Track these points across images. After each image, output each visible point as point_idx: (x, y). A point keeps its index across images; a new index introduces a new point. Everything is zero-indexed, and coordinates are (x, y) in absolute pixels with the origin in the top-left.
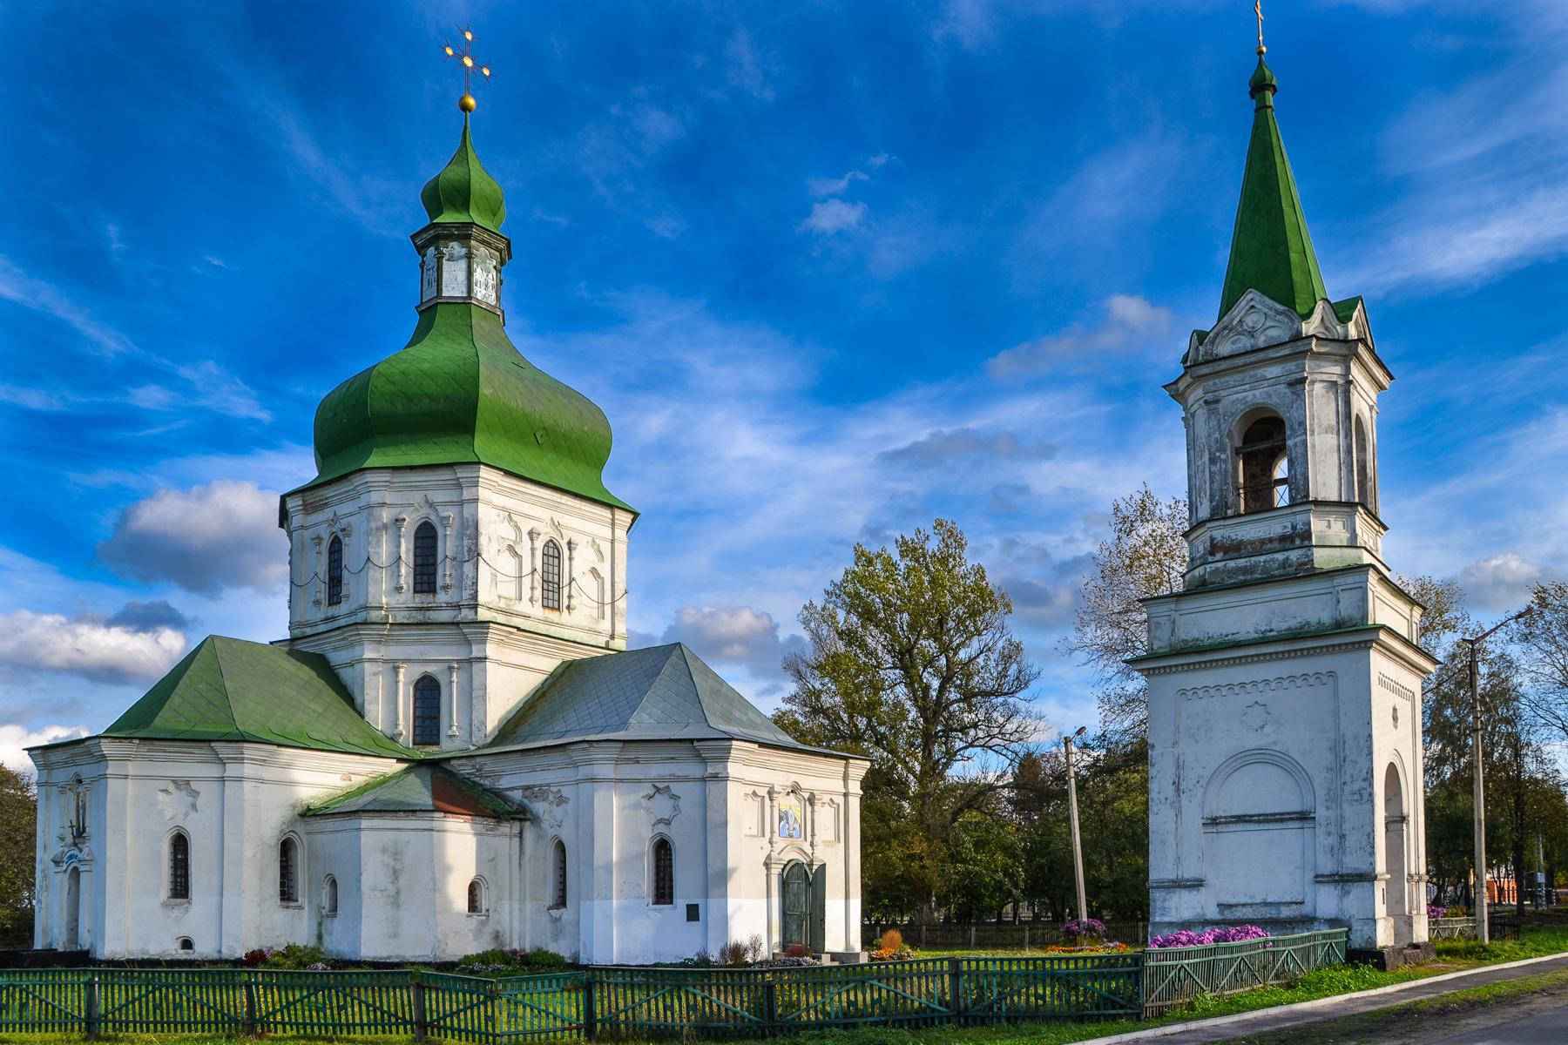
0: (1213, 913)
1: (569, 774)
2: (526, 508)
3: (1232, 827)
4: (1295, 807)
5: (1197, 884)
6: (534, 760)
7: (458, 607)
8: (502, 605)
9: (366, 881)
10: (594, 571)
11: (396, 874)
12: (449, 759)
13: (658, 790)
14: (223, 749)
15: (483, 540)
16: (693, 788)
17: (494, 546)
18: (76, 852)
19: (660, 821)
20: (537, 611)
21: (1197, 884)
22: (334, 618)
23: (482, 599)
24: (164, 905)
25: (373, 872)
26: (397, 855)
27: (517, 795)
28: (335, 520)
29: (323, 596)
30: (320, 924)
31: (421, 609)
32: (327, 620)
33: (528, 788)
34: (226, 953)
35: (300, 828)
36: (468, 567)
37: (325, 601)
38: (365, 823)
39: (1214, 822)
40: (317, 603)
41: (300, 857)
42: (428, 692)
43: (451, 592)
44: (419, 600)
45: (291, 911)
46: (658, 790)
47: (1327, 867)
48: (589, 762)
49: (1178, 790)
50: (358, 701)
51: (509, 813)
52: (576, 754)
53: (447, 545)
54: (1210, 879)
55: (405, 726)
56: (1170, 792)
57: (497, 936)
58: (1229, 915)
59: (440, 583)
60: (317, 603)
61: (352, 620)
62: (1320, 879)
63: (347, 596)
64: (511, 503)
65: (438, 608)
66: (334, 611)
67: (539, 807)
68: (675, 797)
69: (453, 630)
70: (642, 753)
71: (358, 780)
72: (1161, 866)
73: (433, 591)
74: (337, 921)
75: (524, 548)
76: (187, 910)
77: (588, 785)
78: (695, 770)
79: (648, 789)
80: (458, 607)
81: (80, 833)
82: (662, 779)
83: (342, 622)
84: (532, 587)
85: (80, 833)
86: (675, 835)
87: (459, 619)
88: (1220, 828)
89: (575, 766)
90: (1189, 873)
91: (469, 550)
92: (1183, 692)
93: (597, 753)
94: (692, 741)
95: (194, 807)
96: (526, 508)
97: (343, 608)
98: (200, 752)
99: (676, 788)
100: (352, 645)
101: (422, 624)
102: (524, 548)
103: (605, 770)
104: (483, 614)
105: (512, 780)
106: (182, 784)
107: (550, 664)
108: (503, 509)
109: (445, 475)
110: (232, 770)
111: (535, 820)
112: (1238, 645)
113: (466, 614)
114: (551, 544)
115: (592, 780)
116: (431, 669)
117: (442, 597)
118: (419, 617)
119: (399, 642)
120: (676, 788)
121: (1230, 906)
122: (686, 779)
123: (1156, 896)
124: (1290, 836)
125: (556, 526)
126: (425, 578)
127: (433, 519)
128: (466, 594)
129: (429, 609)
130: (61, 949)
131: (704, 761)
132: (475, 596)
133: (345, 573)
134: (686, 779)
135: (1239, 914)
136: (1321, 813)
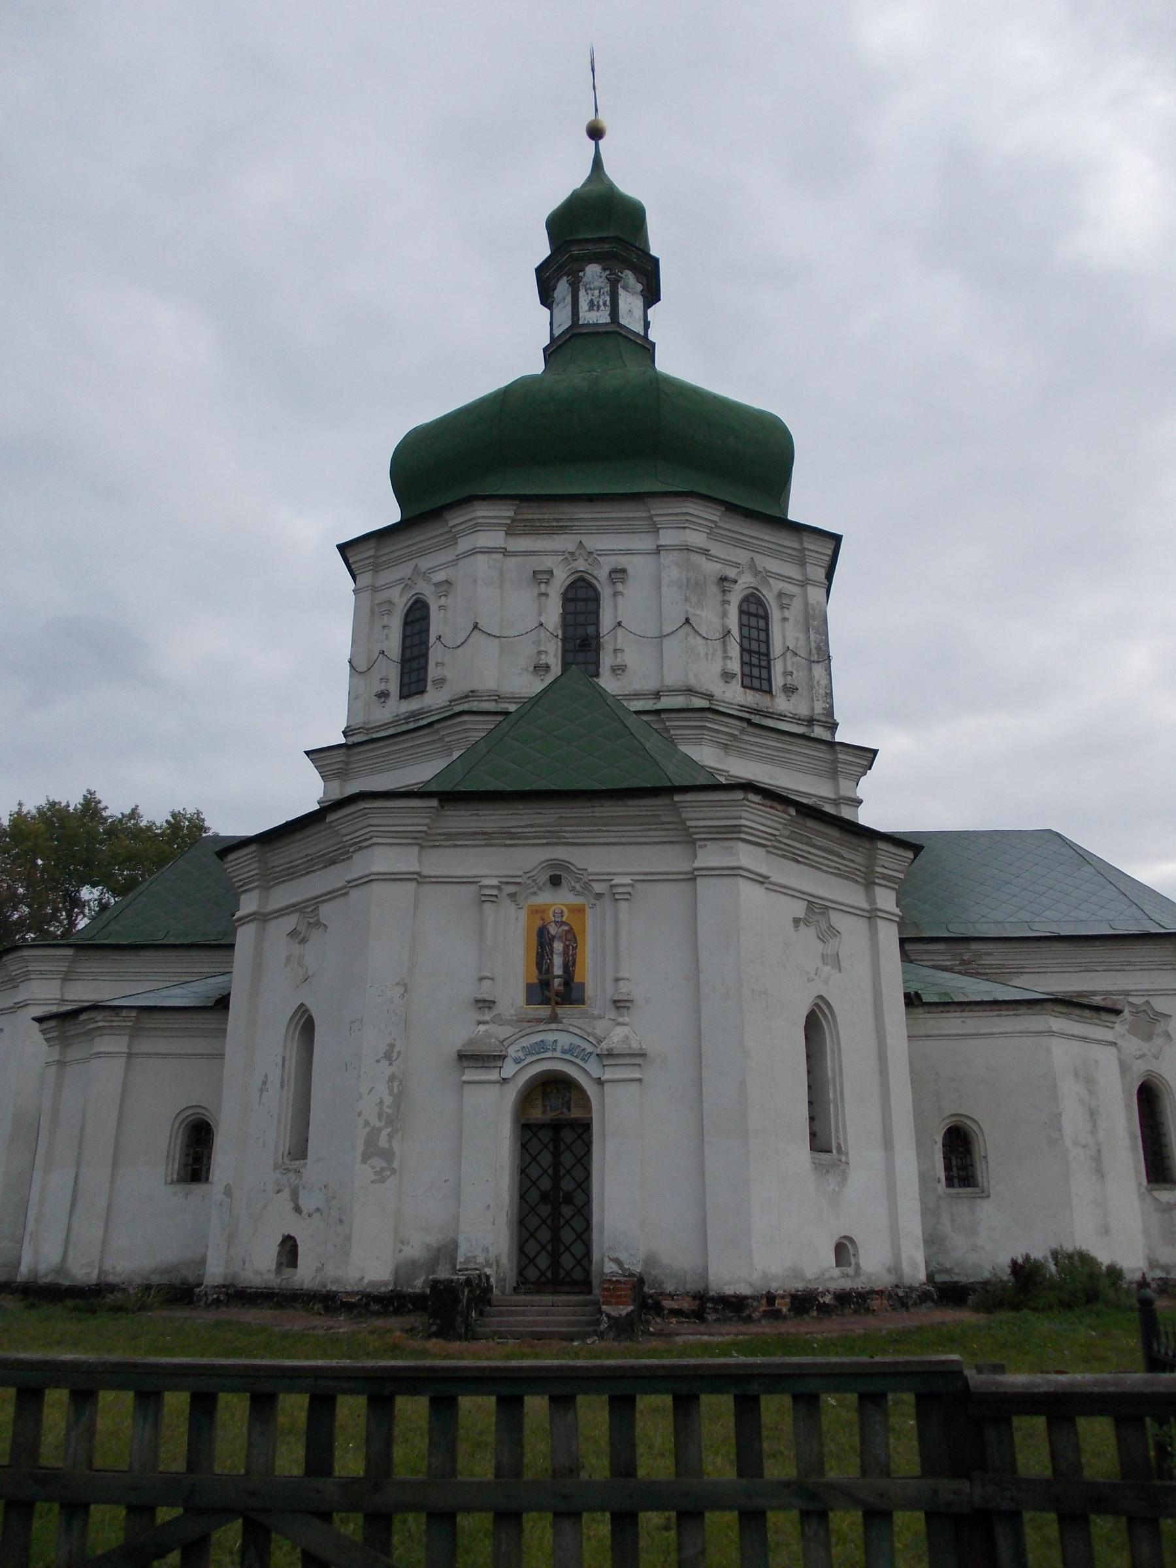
7: (811, 722)
36: (818, 670)
43: (794, 699)
44: (751, 699)
53: (784, 634)
59: (778, 681)
73: (770, 692)
85: (556, 989)
95: (836, 962)
113: (819, 732)
128: (819, 707)
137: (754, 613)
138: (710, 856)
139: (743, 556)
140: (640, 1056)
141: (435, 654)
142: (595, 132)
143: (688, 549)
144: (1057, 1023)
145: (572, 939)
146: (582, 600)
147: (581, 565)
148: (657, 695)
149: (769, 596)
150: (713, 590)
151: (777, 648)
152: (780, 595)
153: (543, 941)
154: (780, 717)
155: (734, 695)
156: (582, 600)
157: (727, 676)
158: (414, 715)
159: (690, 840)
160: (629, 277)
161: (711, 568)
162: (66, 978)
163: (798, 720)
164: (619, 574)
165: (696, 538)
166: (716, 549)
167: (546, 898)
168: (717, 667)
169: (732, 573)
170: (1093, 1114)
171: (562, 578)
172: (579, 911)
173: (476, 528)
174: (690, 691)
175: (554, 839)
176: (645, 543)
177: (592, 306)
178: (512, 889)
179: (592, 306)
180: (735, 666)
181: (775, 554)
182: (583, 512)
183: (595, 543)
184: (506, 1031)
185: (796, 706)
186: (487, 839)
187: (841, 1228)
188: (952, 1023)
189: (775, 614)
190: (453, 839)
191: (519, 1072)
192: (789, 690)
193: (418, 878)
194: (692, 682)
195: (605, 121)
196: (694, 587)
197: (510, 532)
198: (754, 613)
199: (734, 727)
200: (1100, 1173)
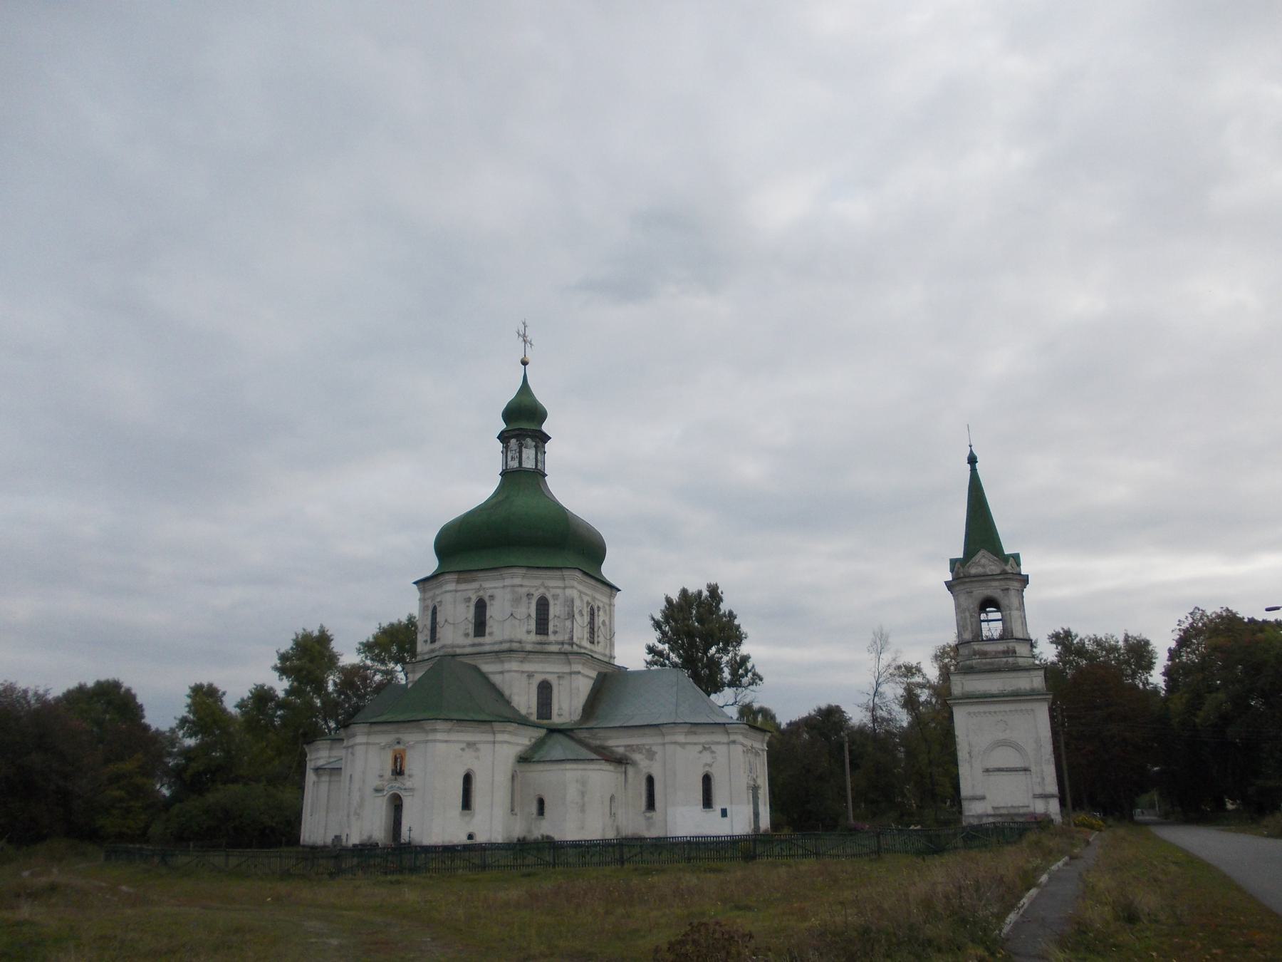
0: (990, 811)
1: (659, 740)
5: (983, 798)
7: (563, 643)
10: (604, 623)
12: (572, 730)
13: (705, 748)
14: (497, 726)
20: (588, 645)
21: (983, 798)
22: (480, 645)
23: (575, 640)
28: (479, 590)
29: (471, 630)
32: (473, 645)
37: (472, 633)
42: (545, 690)
50: (507, 693)
53: (555, 610)
54: (988, 796)
55: (534, 709)
60: (467, 635)
61: (496, 648)
63: (491, 634)
64: (581, 588)
67: (637, 757)
68: (713, 752)
69: (562, 657)
72: (966, 789)
77: (672, 747)
78: (724, 739)
79: (700, 748)
81: (398, 772)
83: (487, 648)
84: (586, 635)
85: (398, 772)
90: (979, 793)
92: (969, 713)
97: (487, 639)
98: (487, 727)
99: (714, 748)
100: (502, 662)
101: (540, 653)
103: (681, 739)
106: (470, 745)
107: (594, 674)
108: (580, 592)
109: (558, 573)
110: (500, 737)
112: (993, 696)
113: (567, 648)
114: (592, 609)
116: (549, 677)
117: (552, 638)
118: (539, 648)
120: (714, 748)
123: (965, 804)
125: (594, 599)
126: (542, 625)
128: (567, 637)
130: (499, 838)
131: (728, 734)
133: (489, 622)
134: (718, 743)
137: (543, 605)
138: (431, 737)
139: (537, 582)
140: (411, 790)
141: (438, 629)
142: (525, 363)
144: (568, 766)
145: (402, 758)
146: (481, 607)
147: (481, 593)
148: (501, 643)
149: (549, 596)
150: (525, 599)
153: (396, 759)
155: (533, 637)
156: (481, 607)
157: (529, 632)
158: (433, 651)
159: (426, 732)
160: (529, 441)
161: (524, 591)
162: (331, 749)
163: (557, 643)
164: (492, 597)
165: (517, 581)
166: (526, 582)
167: (397, 747)
168: (524, 630)
169: (532, 591)
170: (583, 794)
171: (474, 599)
172: (404, 750)
173: (447, 583)
174: (511, 641)
175: (397, 732)
176: (500, 584)
177: (513, 458)
178: (389, 746)
179: (513, 458)
182: (480, 575)
183: (487, 585)
185: (560, 638)
186: (383, 732)
187: (470, 830)
188: (540, 767)
189: (551, 602)
190: (376, 733)
191: (387, 793)
192: (555, 633)
193: (367, 744)
195: (529, 357)
196: (516, 601)
197: (458, 582)
198: (543, 605)
199: (522, 655)
200: (583, 810)
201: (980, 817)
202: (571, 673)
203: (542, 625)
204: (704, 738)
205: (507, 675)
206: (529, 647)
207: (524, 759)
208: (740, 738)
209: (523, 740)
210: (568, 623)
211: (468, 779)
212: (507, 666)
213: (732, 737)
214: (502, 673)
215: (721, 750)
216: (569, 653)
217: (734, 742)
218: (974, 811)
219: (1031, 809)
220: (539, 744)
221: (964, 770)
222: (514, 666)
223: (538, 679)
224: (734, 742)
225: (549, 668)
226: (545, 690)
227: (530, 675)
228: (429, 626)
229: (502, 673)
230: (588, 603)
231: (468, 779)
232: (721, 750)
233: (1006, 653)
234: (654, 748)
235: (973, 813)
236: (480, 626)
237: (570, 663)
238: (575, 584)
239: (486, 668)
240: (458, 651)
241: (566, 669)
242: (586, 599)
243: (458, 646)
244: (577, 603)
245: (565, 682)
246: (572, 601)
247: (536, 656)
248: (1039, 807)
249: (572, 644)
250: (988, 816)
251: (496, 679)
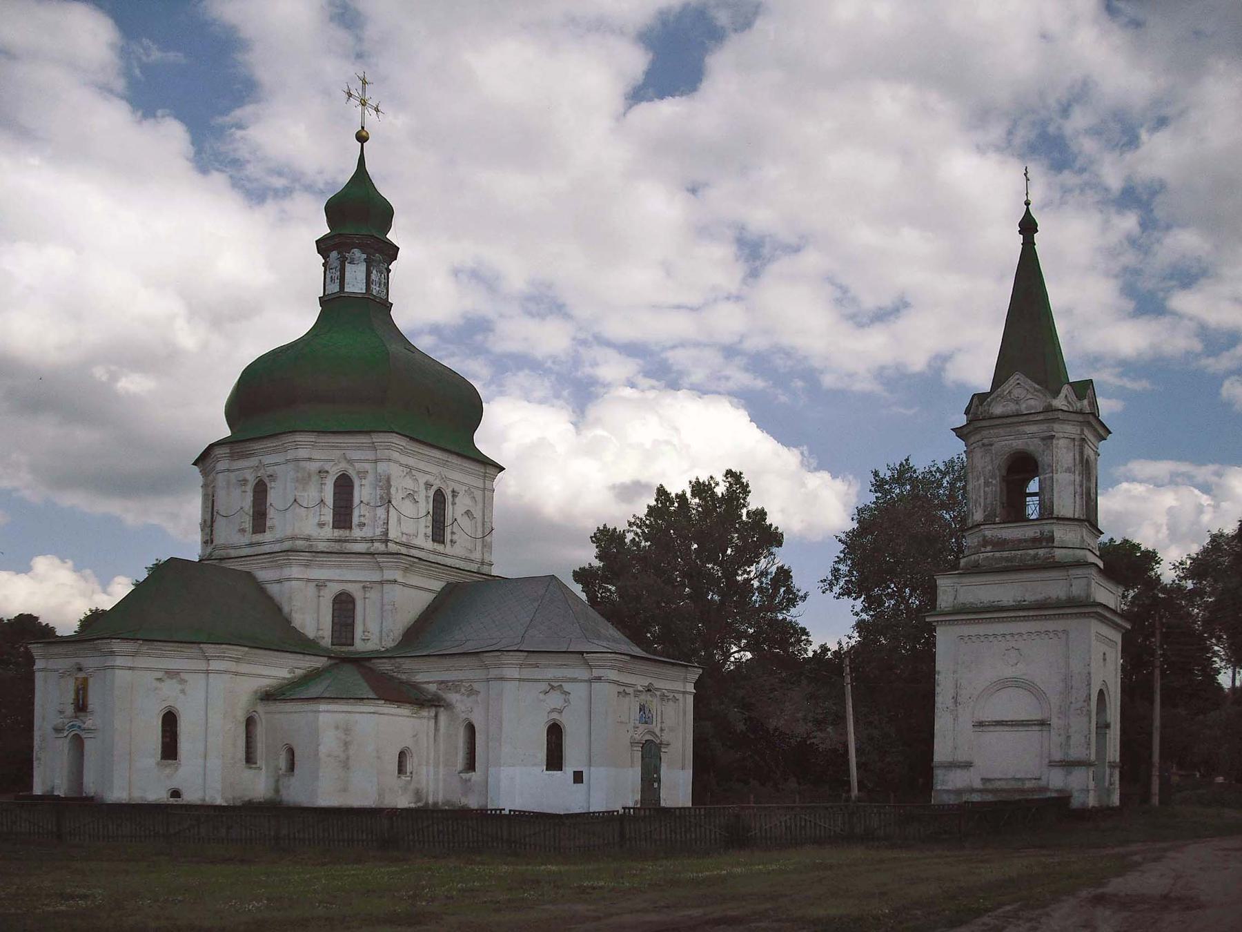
0: (978, 784)
1: (480, 674)
2: (422, 465)
3: (992, 728)
4: (1039, 717)
5: (968, 765)
6: (447, 662)
7: (372, 541)
8: (404, 539)
9: (323, 750)
11: (346, 744)
12: (370, 659)
15: (393, 491)
16: (584, 686)
17: (400, 495)
18: (78, 723)
19: (553, 710)
21: (968, 765)
22: (259, 544)
23: (392, 535)
24: (158, 764)
25: (329, 742)
26: (347, 731)
27: (433, 688)
28: (261, 465)
29: (248, 524)
30: (277, 781)
31: (339, 541)
32: (251, 545)
33: (442, 682)
34: (208, 801)
35: (261, 709)
38: (323, 707)
39: (980, 724)
40: (243, 531)
41: (260, 732)
42: (344, 606)
44: (338, 533)
45: (253, 771)
46: (553, 687)
47: (1057, 756)
48: (499, 666)
49: (956, 702)
50: (286, 609)
51: (429, 701)
52: (488, 659)
53: (363, 493)
56: (950, 703)
57: (418, 793)
58: (989, 786)
59: (355, 520)
60: (243, 531)
61: (277, 548)
62: (1052, 764)
64: (411, 461)
65: (355, 541)
66: (258, 538)
67: (453, 697)
69: (368, 559)
70: (543, 660)
71: (299, 672)
72: (942, 751)
73: (350, 528)
74: (293, 780)
75: (421, 497)
76: (177, 769)
78: (583, 674)
79: (544, 686)
80: (372, 541)
82: (557, 680)
83: (267, 549)
86: (566, 721)
87: (372, 550)
88: (984, 729)
89: (487, 667)
90: (962, 757)
91: (382, 498)
93: (506, 659)
94: (582, 653)
96: (422, 465)
97: (267, 536)
99: (567, 687)
100: (281, 567)
101: (339, 553)
102: (421, 497)
103: (513, 673)
104: (392, 547)
105: (427, 676)
108: (407, 466)
111: (448, 706)
113: (379, 547)
115: (502, 679)
116: (349, 588)
117: (357, 533)
118: (336, 547)
119: (321, 566)
120: (567, 687)
121: (989, 780)
122: (574, 680)
123: (939, 774)
124: (1034, 734)
126: (343, 515)
127: (352, 473)
128: (378, 531)
129: (346, 541)
132: (386, 533)
134: (574, 680)
135: (997, 785)
136: (1055, 721)
143: (297, 460)
151: (356, 501)
152: (359, 473)
154: (355, 541)
155: (328, 532)
163: (364, 540)
180: (328, 517)
181: (359, 448)
184: (66, 721)
185: (367, 532)
188: (289, 707)
192: (362, 525)
194: (297, 531)
199: (307, 556)
201: (959, 792)
202: (381, 583)
203: (343, 515)
204: (550, 673)
205: (287, 584)
206: (322, 546)
207: (269, 696)
208: (613, 675)
209: (278, 669)
210: (381, 512)
211: (170, 721)
212: (286, 572)
213: (596, 673)
214: (279, 581)
215: (578, 692)
216: (384, 552)
217: (599, 679)
218: (950, 783)
219: (1043, 783)
220: (311, 677)
221: (942, 723)
222: (295, 571)
223: (335, 588)
224: (599, 679)
225: (349, 575)
226: (344, 606)
227: (321, 585)
228: (209, 523)
229: (279, 581)
230: (428, 485)
231: (170, 721)
232: (578, 692)
233: (1036, 542)
234: (475, 686)
235: (950, 786)
236: (260, 519)
237: (381, 569)
238: (395, 455)
239: (263, 575)
240: (233, 553)
241: (376, 577)
242: (423, 479)
243: (235, 548)
244: (401, 483)
245: (373, 595)
246: (388, 480)
247: (334, 558)
248: (1056, 780)
249: (386, 541)
250: (973, 790)
251: (273, 589)
